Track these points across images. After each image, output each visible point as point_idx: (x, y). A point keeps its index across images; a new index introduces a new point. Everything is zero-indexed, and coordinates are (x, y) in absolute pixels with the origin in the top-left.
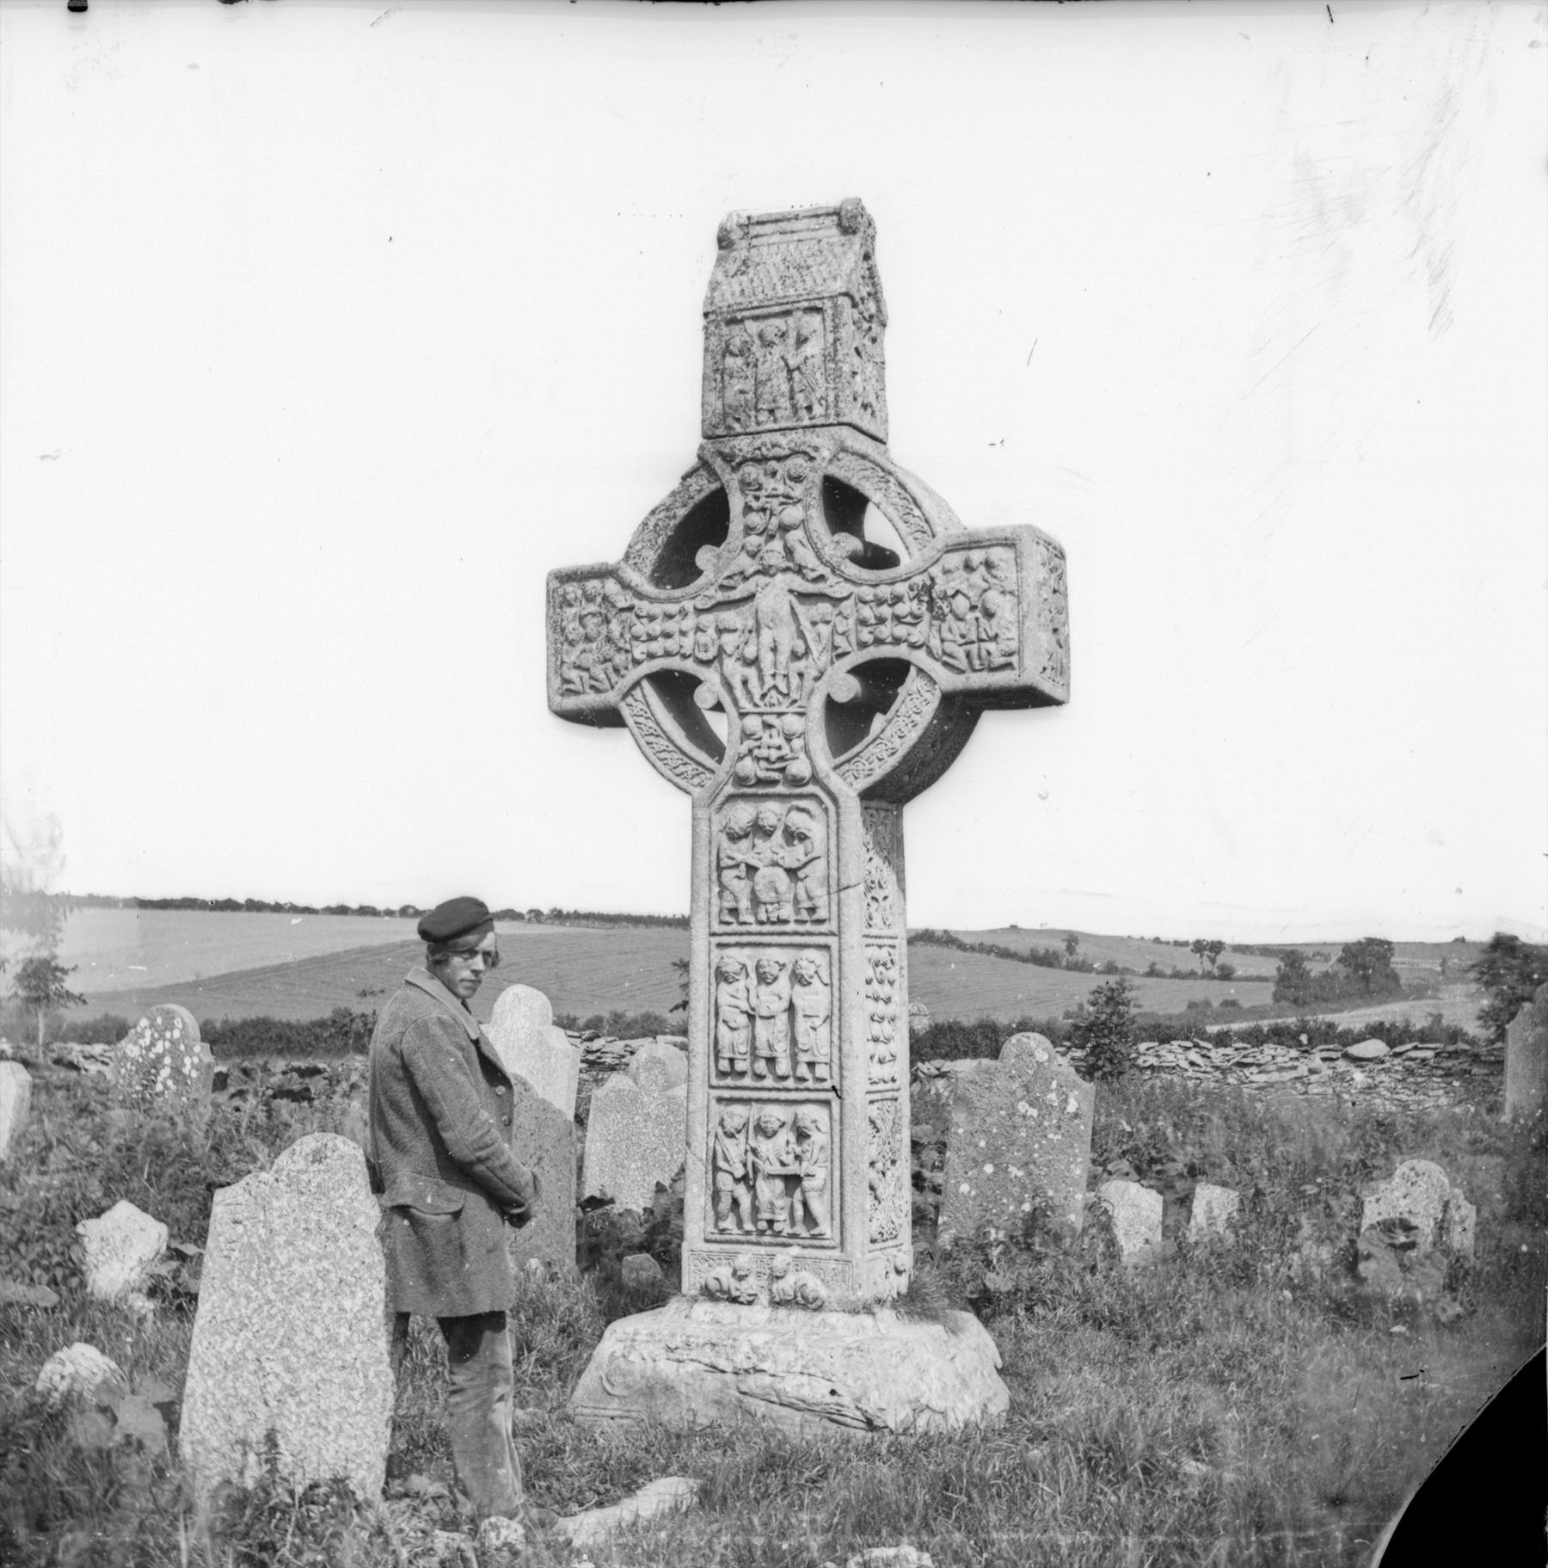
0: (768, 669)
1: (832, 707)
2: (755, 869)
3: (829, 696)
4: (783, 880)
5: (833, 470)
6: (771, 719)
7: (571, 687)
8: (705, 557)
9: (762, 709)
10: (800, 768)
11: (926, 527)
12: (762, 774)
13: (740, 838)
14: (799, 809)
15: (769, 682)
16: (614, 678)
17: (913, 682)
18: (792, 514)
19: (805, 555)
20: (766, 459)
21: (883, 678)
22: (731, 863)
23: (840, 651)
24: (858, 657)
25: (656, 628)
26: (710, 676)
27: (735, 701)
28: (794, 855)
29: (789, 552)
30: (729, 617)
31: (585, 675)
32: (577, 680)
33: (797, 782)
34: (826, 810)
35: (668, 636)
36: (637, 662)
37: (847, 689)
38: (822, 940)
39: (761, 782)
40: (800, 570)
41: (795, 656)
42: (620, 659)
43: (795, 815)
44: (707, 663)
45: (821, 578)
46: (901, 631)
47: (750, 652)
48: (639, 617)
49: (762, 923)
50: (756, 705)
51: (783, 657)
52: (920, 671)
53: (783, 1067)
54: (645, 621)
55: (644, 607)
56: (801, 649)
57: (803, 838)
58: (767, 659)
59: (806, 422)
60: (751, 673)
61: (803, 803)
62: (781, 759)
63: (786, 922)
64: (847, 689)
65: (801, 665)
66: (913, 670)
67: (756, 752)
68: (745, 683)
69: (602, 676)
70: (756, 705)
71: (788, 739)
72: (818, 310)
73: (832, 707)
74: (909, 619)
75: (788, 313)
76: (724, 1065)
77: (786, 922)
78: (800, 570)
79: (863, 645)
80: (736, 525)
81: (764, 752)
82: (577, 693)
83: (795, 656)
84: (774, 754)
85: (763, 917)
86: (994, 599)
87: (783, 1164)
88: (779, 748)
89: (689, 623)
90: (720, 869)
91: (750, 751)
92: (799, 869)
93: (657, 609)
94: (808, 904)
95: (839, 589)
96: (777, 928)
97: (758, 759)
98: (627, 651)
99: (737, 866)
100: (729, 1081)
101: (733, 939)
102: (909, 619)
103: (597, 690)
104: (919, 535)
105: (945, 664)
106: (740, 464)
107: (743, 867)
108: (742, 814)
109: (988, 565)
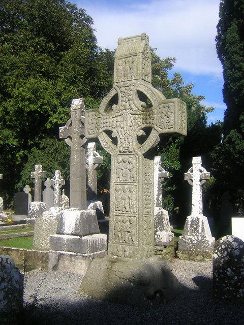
0: (125, 129)
3: (137, 136)
5: (138, 89)
6: (126, 139)
8: (114, 106)
10: (130, 149)
17: (153, 131)
18: (131, 97)
19: (133, 106)
24: (143, 126)
25: (105, 121)
26: (115, 131)
28: (130, 166)
30: (119, 118)
37: (141, 133)
39: (124, 152)
40: (131, 109)
43: (130, 159)
47: (122, 126)
53: (128, 209)
55: (102, 117)
56: (131, 125)
59: (134, 79)
60: (122, 130)
61: (132, 156)
72: (136, 56)
80: (120, 101)
81: (124, 146)
86: (169, 114)
89: (110, 120)
93: (105, 117)
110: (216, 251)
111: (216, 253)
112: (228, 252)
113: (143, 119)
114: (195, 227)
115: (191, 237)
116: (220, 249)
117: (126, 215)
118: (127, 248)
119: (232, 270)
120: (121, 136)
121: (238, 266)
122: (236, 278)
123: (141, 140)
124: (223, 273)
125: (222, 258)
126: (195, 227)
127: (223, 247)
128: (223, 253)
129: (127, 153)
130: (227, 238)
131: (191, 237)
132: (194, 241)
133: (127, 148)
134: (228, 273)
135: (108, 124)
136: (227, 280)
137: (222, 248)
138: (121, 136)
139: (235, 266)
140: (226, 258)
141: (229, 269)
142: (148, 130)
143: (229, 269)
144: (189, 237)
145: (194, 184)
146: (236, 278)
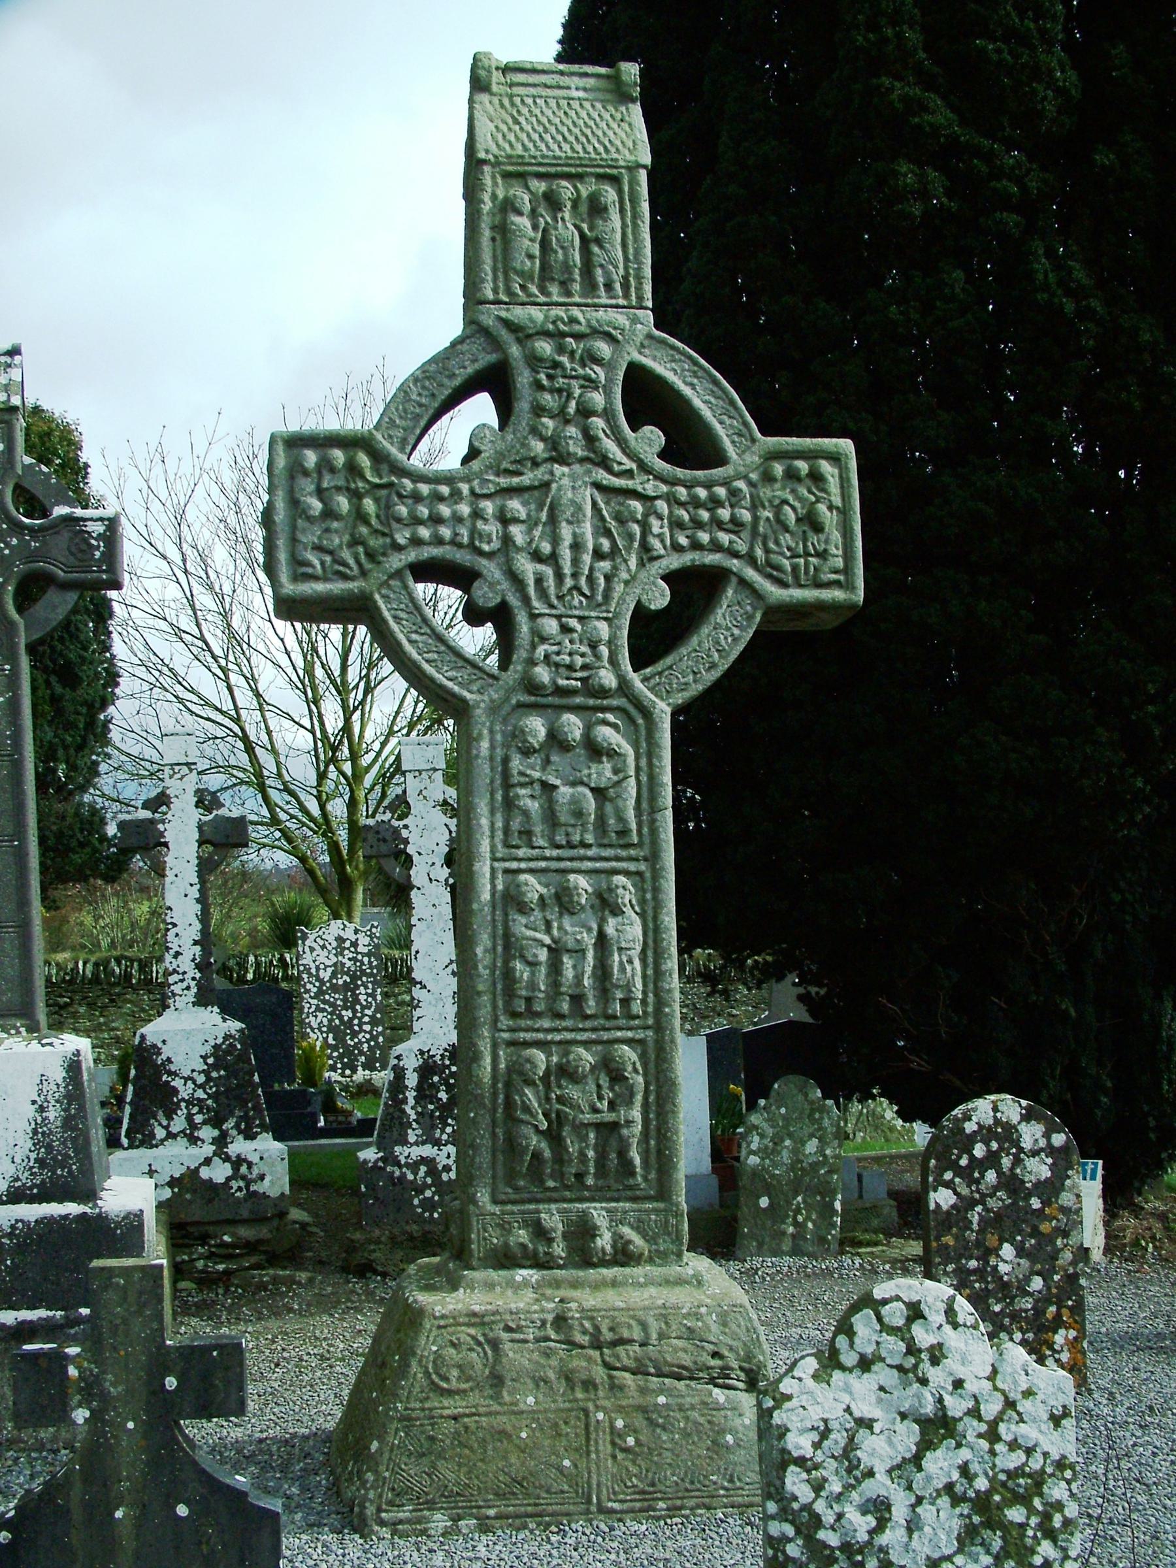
0: (567, 570)
1: (641, 615)
2: (555, 787)
3: (639, 602)
4: (590, 804)
5: (637, 357)
6: (573, 623)
7: (310, 570)
9: (561, 610)
11: (744, 430)
12: (562, 682)
13: (535, 751)
14: (606, 723)
15: (569, 582)
16: (368, 566)
20: (563, 335)
21: (696, 590)
22: (522, 779)
23: (655, 553)
24: (675, 562)
27: (526, 600)
28: (603, 773)
29: (590, 439)
30: (515, 505)
31: (328, 559)
32: (317, 563)
33: (603, 692)
34: (632, 721)
35: (436, 520)
36: (399, 548)
37: (660, 598)
38: (632, 867)
41: (598, 555)
42: (375, 542)
44: (490, 555)
45: (629, 474)
46: (724, 538)
48: (400, 496)
49: (558, 847)
50: (552, 606)
51: (587, 558)
52: (743, 583)
53: (591, 1006)
54: (410, 501)
57: (612, 754)
58: (566, 554)
62: (585, 667)
63: (589, 846)
64: (660, 598)
65: (605, 565)
66: (734, 580)
67: (557, 659)
68: (539, 581)
69: (351, 562)
70: (552, 606)
71: (593, 646)
72: (615, 180)
73: (641, 615)
74: (730, 526)
75: (580, 177)
76: (521, 1007)
77: (589, 846)
78: (604, 462)
79: (677, 548)
82: (315, 578)
83: (598, 555)
84: (579, 661)
85: (560, 839)
87: (596, 1111)
88: (583, 655)
90: (507, 786)
91: (547, 656)
92: (606, 789)
94: (620, 828)
95: (651, 487)
96: (582, 851)
97: (557, 665)
98: (384, 534)
99: (532, 783)
100: (523, 1023)
101: (523, 865)
102: (730, 526)
103: (345, 577)
104: (736, 438)
105: (769, 577)
106: (529, 336)
107: (537, 786)
108: (537, 727)
109: (816, 477)
110: (948, 1175)
111: (948, 1185)
112: (1000, 1173)
113: (677, 524)
114: (443, 1096)
115: (427, 1151)
116: (964, 1162)
117: (585, 1036)
118: (598, 1213)
119: (1020, 1252)
120: (539, 606)
121: (1045, 1227)
122: (1037, 1283)
123: (654, 637)
124: (980, 1273)
125: (972, 1203)
126: (443, 1096)
127: (979, 1151)
128: (977, 1182)
129: (578, 700)
130: (995, 1109)
131: (427, 1151)
132: (447, 1169)
133: (584, 674)
134: (1003, 1268)
135: (446, 532)
136: (998, 1301)
137: (972, 1158)
138: (539, 606)
139: (1035, 1232)
140: (992, 1203)
141: (1007, 1251)
142: (696, 590)
143: (1007, 1251)
144: (416, 1152)
145: (418, 875)
146: (1037, 1283)
